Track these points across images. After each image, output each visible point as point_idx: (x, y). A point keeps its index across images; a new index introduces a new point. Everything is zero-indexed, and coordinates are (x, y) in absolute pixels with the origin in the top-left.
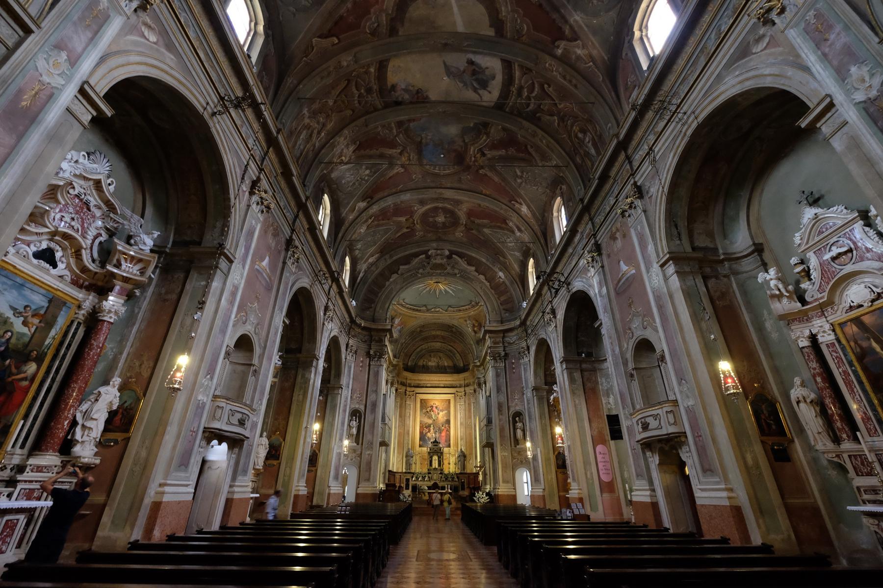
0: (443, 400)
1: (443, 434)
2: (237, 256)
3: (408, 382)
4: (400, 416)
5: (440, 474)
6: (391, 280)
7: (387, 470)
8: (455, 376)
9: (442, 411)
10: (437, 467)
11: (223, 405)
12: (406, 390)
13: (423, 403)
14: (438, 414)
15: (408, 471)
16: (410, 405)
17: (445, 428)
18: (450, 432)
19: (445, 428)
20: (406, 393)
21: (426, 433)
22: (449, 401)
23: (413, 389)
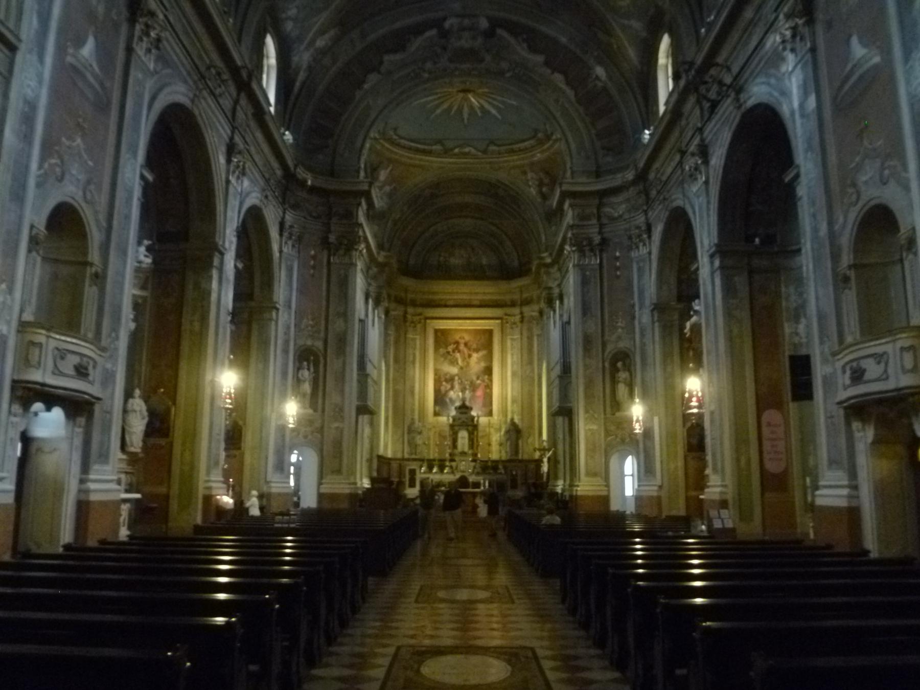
0: (477, 332)
1: (479, 393)
2: (23, 36)
3: (410, 296)
4: (396, 361)
6: (366, 86)
7: (374, 455)
8: (504, 286)
10: (466, 449)
11: (43, 339)
13: (442, 338)
14: (470, 356)
16: (414, 340)
17: (483, 381)
18: (491, 389)
21: (447, 392)
22: (490, 333)
23: (420, 310)
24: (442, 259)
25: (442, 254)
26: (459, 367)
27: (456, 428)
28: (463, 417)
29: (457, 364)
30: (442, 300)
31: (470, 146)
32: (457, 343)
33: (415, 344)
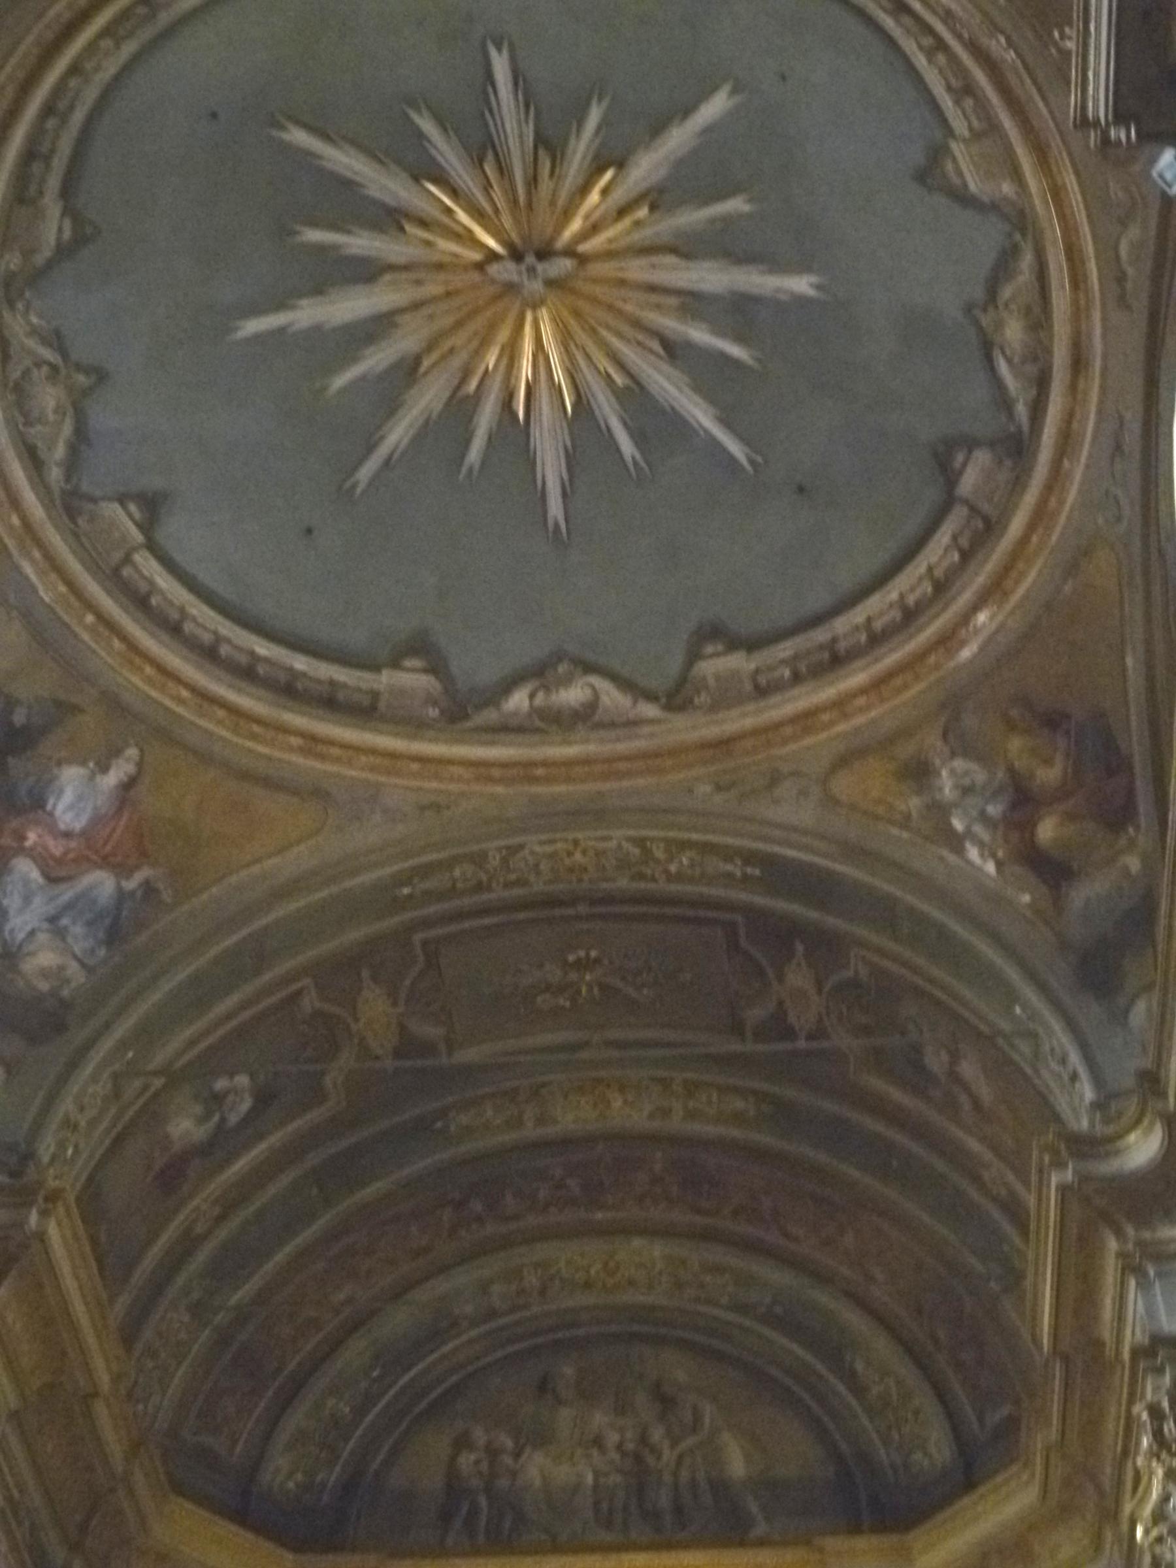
24: (466, 1460)
25: (479, 1435)
31: (590, 668)
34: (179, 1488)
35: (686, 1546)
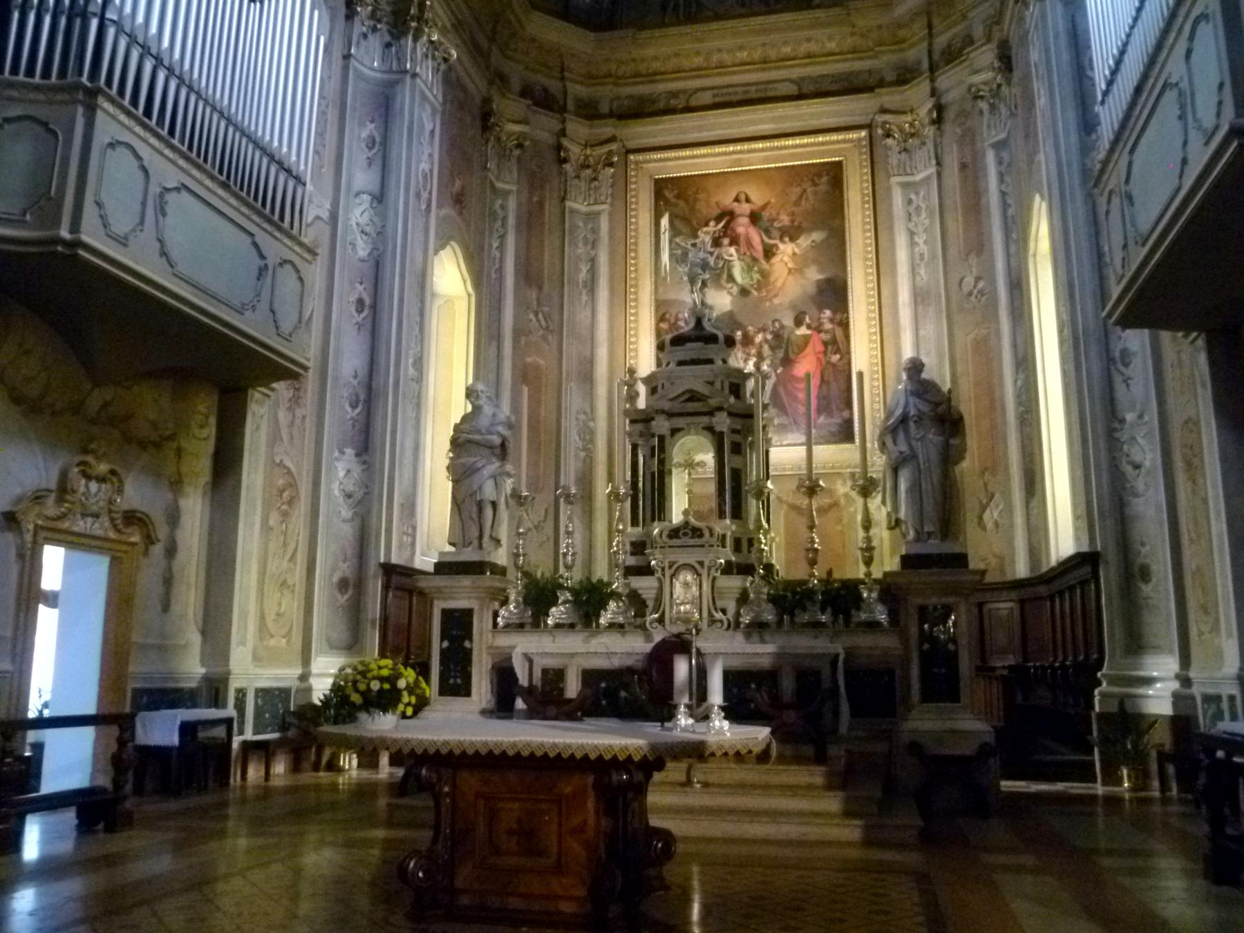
0: (794, 175)
1: (806, 365)
3: (576, 90)
4: (529, 275)
5: (728, 569)
9: (792, 233)
12: (563, 133)
14: (769, 253)
15: (470, 555)
16: (593, 217)
17: (819, 330)
18: (846, 354)
19: (819, 330)
20: (559, 147)
22: (834, 174)
26: (735, 290)
27: (661, 425)
28: (694, 378)
29: (731, 278)
30: (674, 94)
32: (728, 216)
33: (595, 231)
34: (536, 7)
35: (782, 11)
